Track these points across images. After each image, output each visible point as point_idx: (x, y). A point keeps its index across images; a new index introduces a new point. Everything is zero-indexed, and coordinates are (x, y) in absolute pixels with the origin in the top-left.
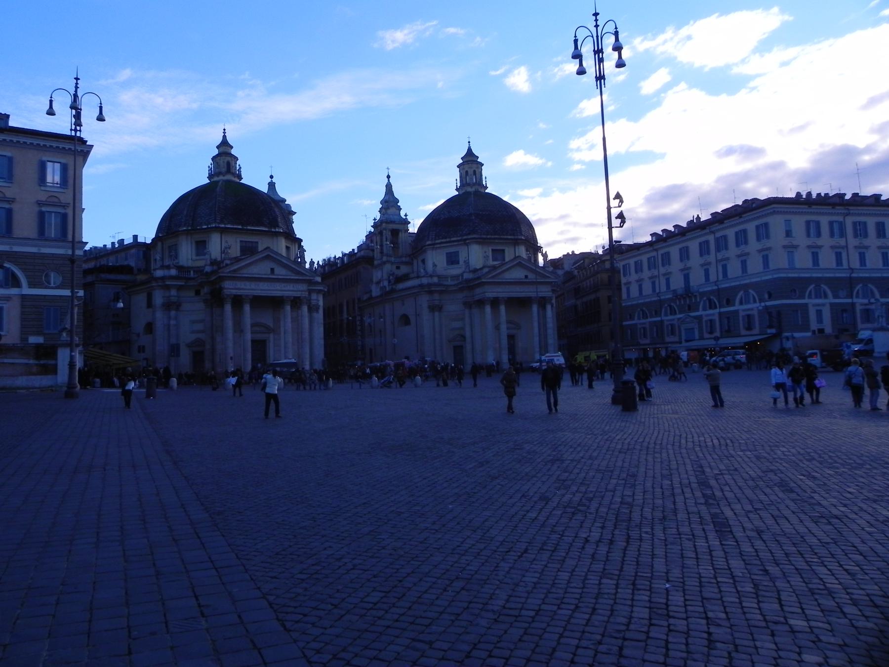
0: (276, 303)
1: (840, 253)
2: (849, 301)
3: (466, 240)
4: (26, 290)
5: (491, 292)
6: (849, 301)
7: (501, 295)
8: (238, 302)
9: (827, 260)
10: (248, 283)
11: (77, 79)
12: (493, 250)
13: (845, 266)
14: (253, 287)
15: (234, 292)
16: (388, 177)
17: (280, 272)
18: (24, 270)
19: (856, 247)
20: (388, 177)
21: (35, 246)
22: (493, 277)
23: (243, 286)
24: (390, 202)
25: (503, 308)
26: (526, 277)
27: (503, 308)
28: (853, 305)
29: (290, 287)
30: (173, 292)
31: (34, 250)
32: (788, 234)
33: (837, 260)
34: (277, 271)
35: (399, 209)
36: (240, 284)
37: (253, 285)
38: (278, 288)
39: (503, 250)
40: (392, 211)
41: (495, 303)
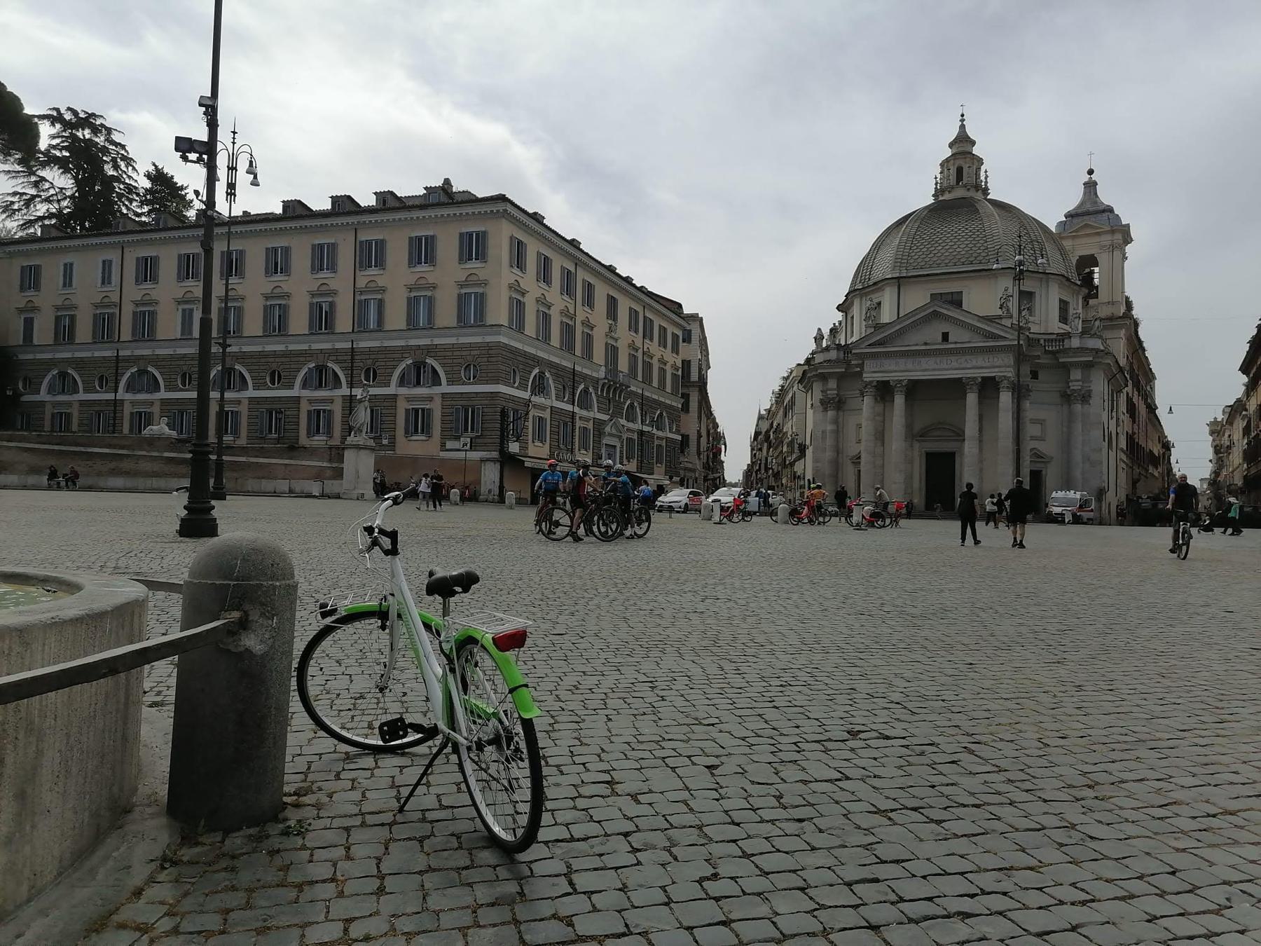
0: (956, 388)
4: (445, 388)
8: (884, 391)
10: (902, 361)
11: (234, 133)
14: (910, 366)
17: (959, 336)
21: (426, 337)
23: (893, 367)
29: (979, 361)
30: (832, 384)
31: (453, 340)
34: (951, 339)
36: (890, 364)
37: (910, 364)
38: (955, 364)
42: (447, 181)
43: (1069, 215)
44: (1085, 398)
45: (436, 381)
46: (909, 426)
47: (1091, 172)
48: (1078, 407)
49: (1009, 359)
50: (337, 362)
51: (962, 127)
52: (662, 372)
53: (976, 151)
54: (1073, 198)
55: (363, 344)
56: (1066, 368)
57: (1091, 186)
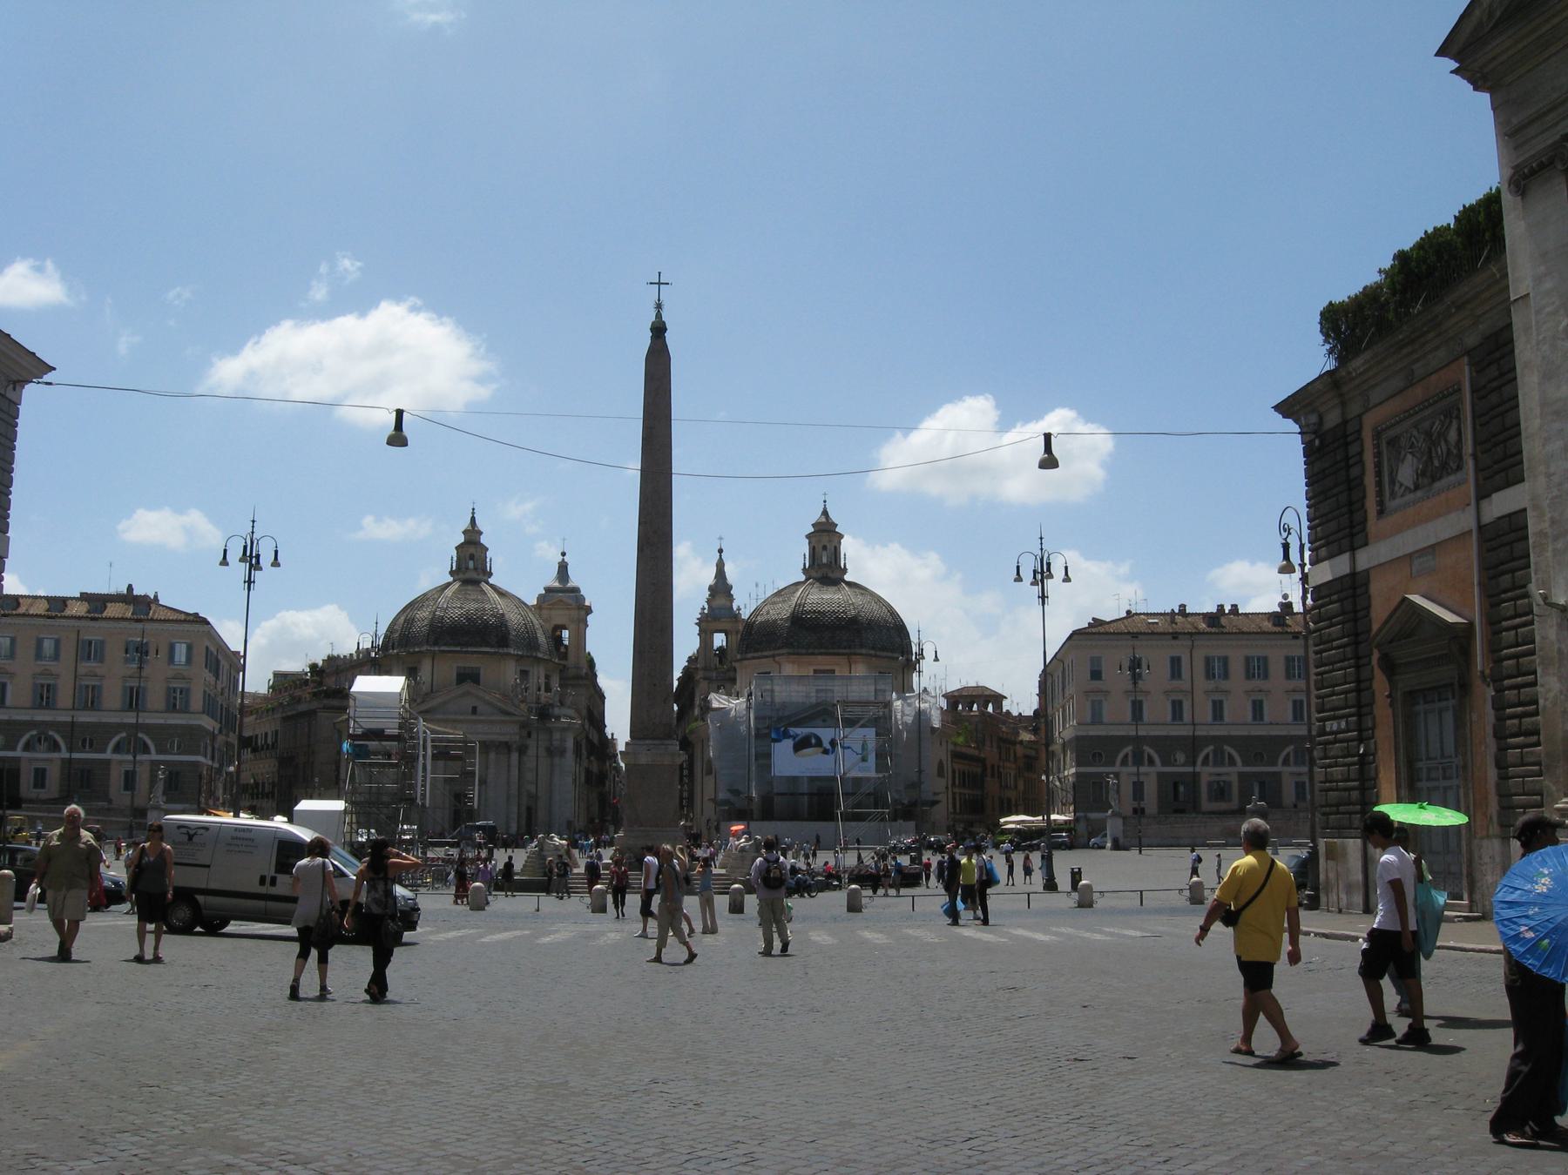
1: (1180, 702)
2: (1190, 769)
4: (154, 756)
6: (1190, 769)
9: (1157, 711)
13: (1187, 717)
16: (721, 551)
18: (152, 739)
19: (1207, 692)
20: (721, 551)
24: (721, 588)
28: (1196, 775)
32: (1096, 675)
33: (1214, 711)
35: (730, 598)
40: (720, 601)
42: (130, 588)
44: (562, 752)
45: (146, 750)
47: (564, 554)
48: (557, 760)
49: (516, 728)
50: (58, 732)
51: (473, 519)
53: (483, 540)
54: (550, 579)
55: (82, 719)
57: (563, 569)
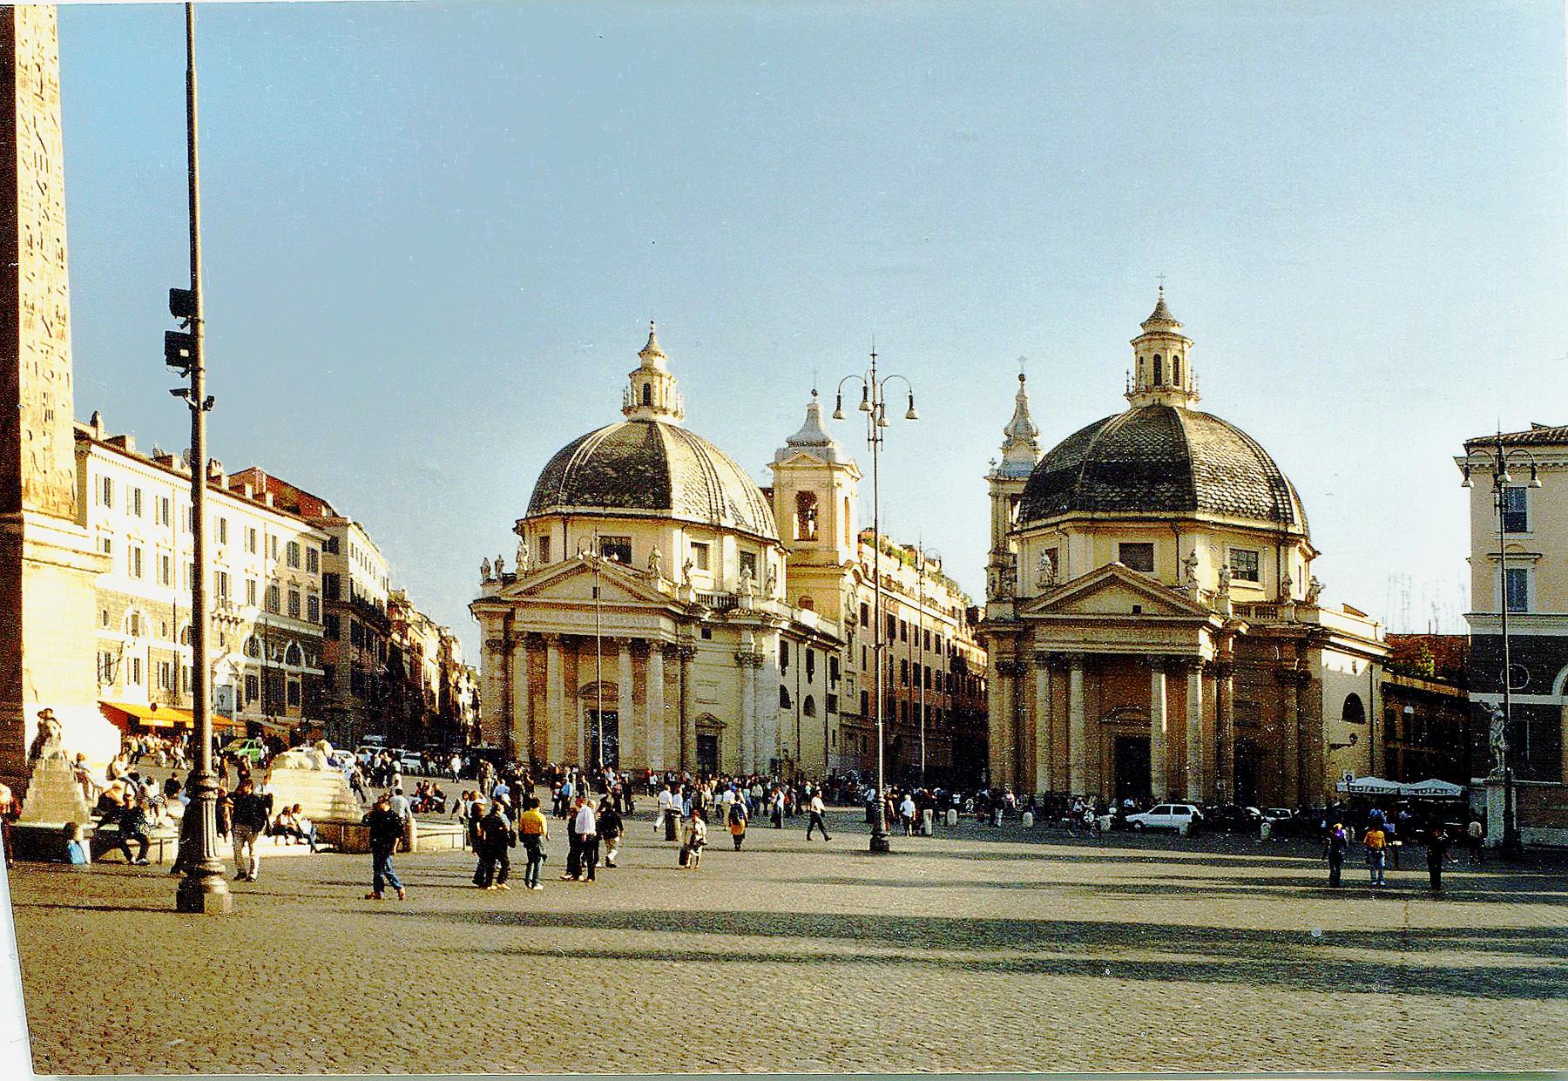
3: (1057, 524)
5: (1048, 641)
7: (1070, 648)
12: (1121, 545)
15: (531, 628)
16: (1022, 378)
22: (1054, 607)
24: (1020, 433)
25: (1076, 676)
26: (1137, 610)
27: (1076, 676)
34: (603, 594)
36: (540, 614)
37: (561, 616)
39: (1148, 548)
41: (1058, 664)
43: (791, 443)
46: (571, 681)
52: (294, 596)
56: (737, 629)
